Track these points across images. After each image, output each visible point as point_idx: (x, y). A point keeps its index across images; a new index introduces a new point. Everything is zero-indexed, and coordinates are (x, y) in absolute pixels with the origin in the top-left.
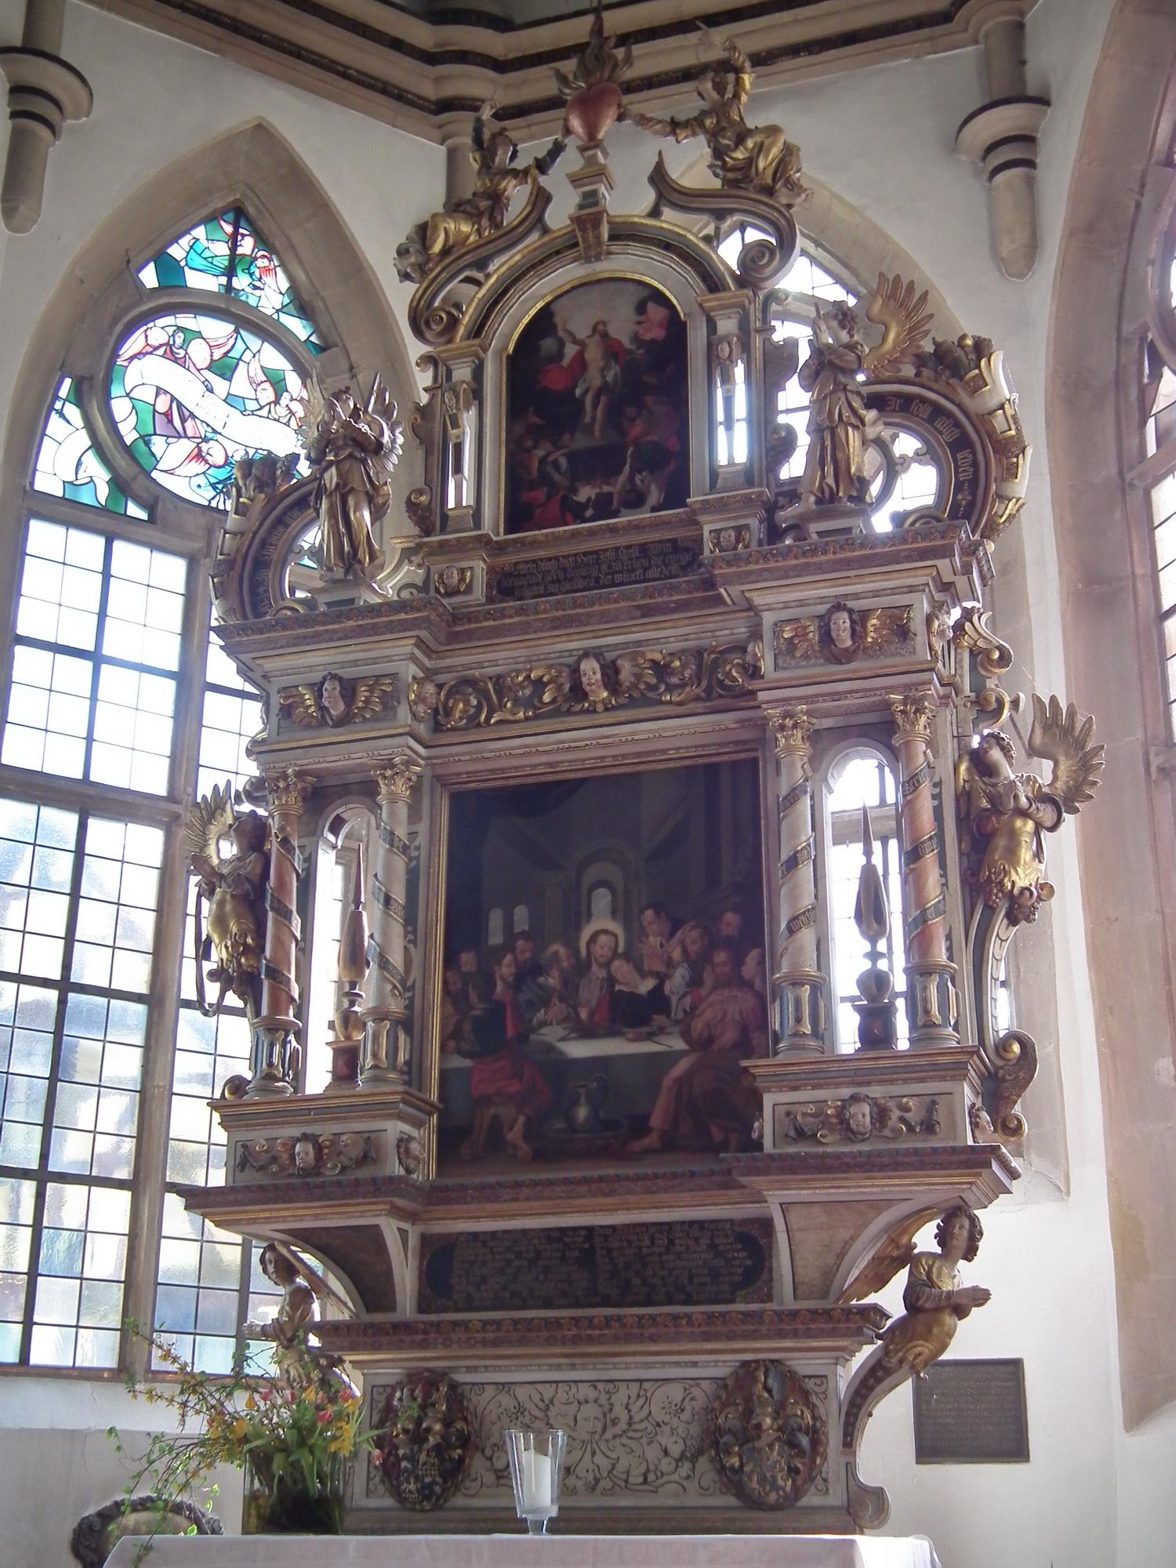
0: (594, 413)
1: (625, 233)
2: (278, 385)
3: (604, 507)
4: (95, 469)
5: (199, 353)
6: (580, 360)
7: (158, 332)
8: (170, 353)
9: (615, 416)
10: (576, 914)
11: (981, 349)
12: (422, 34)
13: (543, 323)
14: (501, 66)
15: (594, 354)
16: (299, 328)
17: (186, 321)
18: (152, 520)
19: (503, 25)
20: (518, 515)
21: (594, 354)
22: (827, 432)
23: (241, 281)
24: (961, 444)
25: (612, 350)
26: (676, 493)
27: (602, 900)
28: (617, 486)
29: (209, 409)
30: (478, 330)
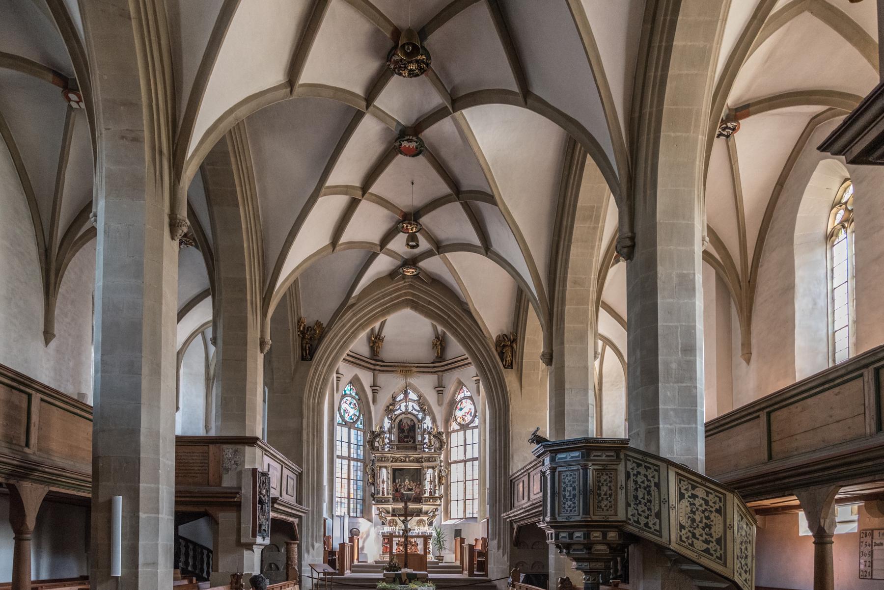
0: (406, 431)
1: (410, 413)
2: (355, 404)
3: (407, 442)
4: (340, 419)
5: (348, 402)
6: (405, 425)
7: (344, 400)
8: (346, 403)
9: (408, 432)
10: (405, 481)
11: (443, 433)
12: (373, 362)
13: (401, 421)
14: (381, 366)
15: (406, 425)
16: (357, 397)
17: (347, 398)
18: (345, 424)
19: (383, 361)
20: (399, 441)
21: (406, 425)
22: (429, 439)
23: (351, 392)
24: (441, 442)
25: (408, 425)
26: (414, 442)
27: (407, 480)
28: (408, 440)
29: (349, 409)
30: (394, 422)
